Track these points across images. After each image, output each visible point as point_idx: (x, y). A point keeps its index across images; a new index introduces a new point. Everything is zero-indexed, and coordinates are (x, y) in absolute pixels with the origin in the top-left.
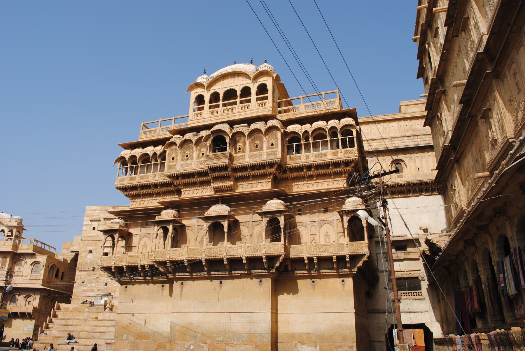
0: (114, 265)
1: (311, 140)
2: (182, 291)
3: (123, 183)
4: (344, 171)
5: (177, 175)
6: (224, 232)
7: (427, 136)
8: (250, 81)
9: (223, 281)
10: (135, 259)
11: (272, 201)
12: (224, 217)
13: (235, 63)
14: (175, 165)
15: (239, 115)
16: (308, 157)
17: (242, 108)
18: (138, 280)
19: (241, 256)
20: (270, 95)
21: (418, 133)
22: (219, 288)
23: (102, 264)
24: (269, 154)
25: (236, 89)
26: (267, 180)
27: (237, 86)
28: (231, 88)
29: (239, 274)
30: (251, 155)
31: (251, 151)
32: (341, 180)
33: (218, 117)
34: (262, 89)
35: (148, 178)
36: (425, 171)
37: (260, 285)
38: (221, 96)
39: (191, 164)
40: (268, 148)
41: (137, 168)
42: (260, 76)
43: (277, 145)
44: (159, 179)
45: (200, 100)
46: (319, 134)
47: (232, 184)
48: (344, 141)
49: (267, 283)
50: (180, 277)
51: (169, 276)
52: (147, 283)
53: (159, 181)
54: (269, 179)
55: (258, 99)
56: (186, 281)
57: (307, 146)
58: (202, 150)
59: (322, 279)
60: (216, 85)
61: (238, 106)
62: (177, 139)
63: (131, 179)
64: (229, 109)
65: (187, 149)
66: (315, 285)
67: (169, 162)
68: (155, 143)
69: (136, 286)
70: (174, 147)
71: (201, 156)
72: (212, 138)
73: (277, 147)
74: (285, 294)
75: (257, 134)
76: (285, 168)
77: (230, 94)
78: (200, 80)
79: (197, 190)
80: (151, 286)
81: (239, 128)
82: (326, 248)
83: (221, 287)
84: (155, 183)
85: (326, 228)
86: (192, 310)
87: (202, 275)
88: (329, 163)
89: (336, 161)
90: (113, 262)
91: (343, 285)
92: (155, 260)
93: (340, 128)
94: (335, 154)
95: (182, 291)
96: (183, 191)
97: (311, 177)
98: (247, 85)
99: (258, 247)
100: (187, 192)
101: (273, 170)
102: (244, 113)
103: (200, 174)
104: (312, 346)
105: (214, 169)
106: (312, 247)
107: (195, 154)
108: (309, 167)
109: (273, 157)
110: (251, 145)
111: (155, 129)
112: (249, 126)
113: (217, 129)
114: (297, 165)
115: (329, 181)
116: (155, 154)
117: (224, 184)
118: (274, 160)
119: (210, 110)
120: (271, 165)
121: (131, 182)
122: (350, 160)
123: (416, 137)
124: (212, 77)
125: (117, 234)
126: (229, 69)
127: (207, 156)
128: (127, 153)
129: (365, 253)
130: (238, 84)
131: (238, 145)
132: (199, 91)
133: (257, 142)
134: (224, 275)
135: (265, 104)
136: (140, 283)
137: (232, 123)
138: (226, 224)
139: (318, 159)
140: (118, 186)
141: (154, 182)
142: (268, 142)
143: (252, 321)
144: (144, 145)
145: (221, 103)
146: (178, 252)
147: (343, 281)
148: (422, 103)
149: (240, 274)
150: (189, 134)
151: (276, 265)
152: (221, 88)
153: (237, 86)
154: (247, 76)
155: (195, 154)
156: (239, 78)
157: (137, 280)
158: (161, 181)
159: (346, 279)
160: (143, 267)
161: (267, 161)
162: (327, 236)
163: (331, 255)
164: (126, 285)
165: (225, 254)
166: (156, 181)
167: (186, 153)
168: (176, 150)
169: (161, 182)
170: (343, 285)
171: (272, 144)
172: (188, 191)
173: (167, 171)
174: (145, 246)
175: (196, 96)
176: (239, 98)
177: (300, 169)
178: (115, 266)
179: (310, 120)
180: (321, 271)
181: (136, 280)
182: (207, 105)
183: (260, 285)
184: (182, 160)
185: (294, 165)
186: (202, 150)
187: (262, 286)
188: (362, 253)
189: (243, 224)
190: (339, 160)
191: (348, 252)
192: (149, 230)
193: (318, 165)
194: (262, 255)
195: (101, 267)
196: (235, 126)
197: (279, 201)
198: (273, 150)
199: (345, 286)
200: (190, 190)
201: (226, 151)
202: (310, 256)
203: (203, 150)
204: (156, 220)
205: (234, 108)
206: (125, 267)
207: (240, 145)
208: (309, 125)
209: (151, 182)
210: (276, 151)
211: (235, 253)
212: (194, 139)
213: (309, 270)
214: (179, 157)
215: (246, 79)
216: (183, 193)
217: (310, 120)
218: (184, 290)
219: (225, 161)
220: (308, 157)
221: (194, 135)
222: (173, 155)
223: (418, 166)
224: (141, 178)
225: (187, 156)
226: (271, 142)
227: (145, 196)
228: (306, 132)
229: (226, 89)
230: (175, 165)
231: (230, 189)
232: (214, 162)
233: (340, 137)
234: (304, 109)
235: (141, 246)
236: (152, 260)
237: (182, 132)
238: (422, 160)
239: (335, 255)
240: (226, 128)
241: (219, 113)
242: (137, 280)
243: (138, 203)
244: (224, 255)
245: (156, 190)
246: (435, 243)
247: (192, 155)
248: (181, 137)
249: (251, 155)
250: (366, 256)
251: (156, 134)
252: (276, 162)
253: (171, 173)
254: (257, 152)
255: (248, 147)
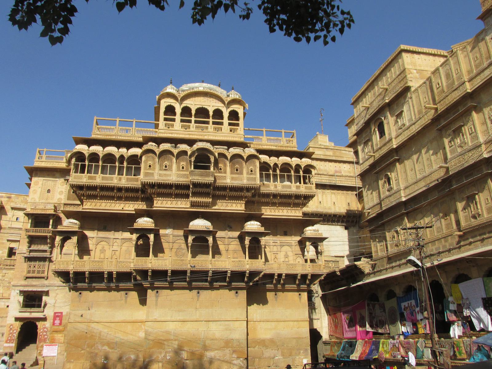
0: (73, 270)
1: (278, 172)
2: (157, 301)
3: (76, 180)
4: (303, 203)
5: (155, 183)
6: (208, 246)
7: (328, 176)
8: (223, 105)
9: (201, 291)
10: (100, 264)
11: (252, 222)
12: (209, 233)
13: (203, 82)
14: (153, 174)
15: (213, 136)
16: (276, 186)
17: (215, 129)
18: (98, 287)
19: (227, 270)
20: (241, 122)
21: (321, 173)
22: (196, 298)
23: (57, 268)
24: (248, 179)
25: (208, 109)
26: (242, 202)
27: (210, 106)
28: (204, 106)
29: (218, 285)
30: (232, 177)
31: (232, 173)
32: (298, 210)
33: (190, 132)
34: (234, 115)
35: (112, 180)
36: (325, 205)
37: (237, 296)
38: (193, 112)
39: (170, 175)
40: (248, 173)
41: (96, 167)
42: (232, 103)
43: (255, 172)
44: (126, 183)
45: (170, 110)
46: (286, 168)
47: (211, 200)
48: (305, 178)
49: (243, 294)
50: (157, 286)
51: (144, 284)
52: (109, 289)
53: (125, 186)
54: (243, 201)
55: (230, 124)
56: (161, 290)
57: (275, 176)
58: (181, 164)
59: (284, 293)
60: (188, 100)
61: (211, 126)
62: (151, 145)
63: (90, 178)
64: (200, 127)
65: (165, 159)
66: (277, 297)
67: (145, 169)
68: (119, 144)
69: (95, 293)
70: (151, 154)
71: (181, 169)
72: (196, 154)
73: (255, 174)
74: (255, 304)
75: (237, 158)
76: (256, 193)
77: (202, 112)
78: (170, 89)
79: (171, 201)
80: (114, 293)
81: (220, 149)
82: (293, 267)
83: (198, 297)
84: (121, 187)
85: (286, 248)
86: (169, 318)
87: (181, 285)
88: (293, 195)
89: (299, 194)
90: (72, 266)
91: (300, 298)
92: (135, 269)
93: (304, 166)
94: (298, 187)
95: (157, 301)
96: (156, 200)
97: (274, 204)
98: (219, 108)
99: (242, 263)
100: (160, 202)
101: (249, 194)
102: (218, 134)
103: (179, 186)
104: (275, 350)
105: (196, 185)
106: (281, 265)
107: (174, 166)
108: (275, 196)
109: (253, 183)
110: (232, 167)
111: (112, 127)
112: (228, 150)
113: (201, 147)
114: (267, 192)
115: (288, 209)
116: (122, 157)
117: (203, 200)
118: (254, 186)
119: (182, 123)
120: (248, 189)
121: (91, 181)
122: (308, 195)
123: (320, 176)
124: (183, 91)
125: (77, 237)
126: (200, 87)
127: (192, 171)
128: (82, 148)
129: (324, 273)
130: (211, 105)
131: (220, 165)
132: (169, 101)
133: (237, 166)
134: (203, 286)
135: (236, 129)
136: (99, 290)
137: (214, 143)
138: (210, 239)
139: (285, 189)
140: (74, 183)
141: (120, 185)
142: (248, 168)
143: (229, 329)
144: (104, 143)
145: (193, 119)
146: (160, 262)
147: (300, 295)
148: (325, 148)
149: (219, 285)
150: (165, 144)
151: (255, 280)
152: (194, 104)
153: (210, 106)
154: (220, 99)
155: (174, 166)
156: (211, 99)
157: (97, 287)
158: (129, 185)
159: (302, 293)
160: (110, 274)
161: (247, 185)
162: (286, 256)
163: (297, 273)
164: (80, 292)
165: (210, 267)
166: (123, 185)
167: (165, 163)
168: (154, 159)
169: (128, 187)
170: (300, 298)
171: (252, 171)
172: (161, 200)
173: (142, 177)
174: (103, 251)
175: (166, 106)
176: (211, 118)
177: (267, 195)
178: (75, 270)
179: (277, 154)
180: (286, 286)
181: (96, 286)
182: (178, 117)
183: (237, 296)
184: (160, 170)
185: (264, 191)
186: (182, 163)
187: (238, 297)
188: (321, 273)
189: (219, 239)
190: (302, 193)
191: (311, 272)
192: (107, 234)
193: (284, 194)
194: (247, 270)
195: (55, 272)
196: (215, 146)
197: (259, 223)
198: (251, 176)
199: (302, 299)
200: (163, 200)
201: (210, 169)
202: (280, 273)
203: (183, 163)
204: (135, 227)
205: (207, 128)
206: (88, 272)
207: (220, 165)
208: (276, 158)
209: (116, 185)
210: (255, 178)
211: (220, 266)
212: (175, 151)
213: (276, 285)
214: (157, 166)
215: (218, 102)
216: (155, 202)
217: (277, 154)
218: (159, 300)
219: (210, 180)
220: (276, 186)
221: (172, 147)
222: (150, 162)
223: (320, 200)
224: (103, 178)
225: (166, 167)
226: (250, 168)
227: (103, 198)
228: (276, 165)
229: (199, 106)
230: (153, 174)
231: (206, 205)
232: (200, 178)
233: (301, 173)
234: (267, 142)
235: (98, 250)
236: (131, 268)
237: (159, 141)
238: (323, 195)
239: (300, 273)
240: (208, 146)
241: (192, 129)
242: (97, 287)
243: (94, 204)
244: (210, 268)
245: (119, 194)
246: (361, 268)
247: (171, 166)
248: (157, 145)
249: (232, 177)
250: (323, 276)
251: (113, 133)
252: (255, 187)
253: (149, 181)
254: (238, 175)
255: (228, 169)
